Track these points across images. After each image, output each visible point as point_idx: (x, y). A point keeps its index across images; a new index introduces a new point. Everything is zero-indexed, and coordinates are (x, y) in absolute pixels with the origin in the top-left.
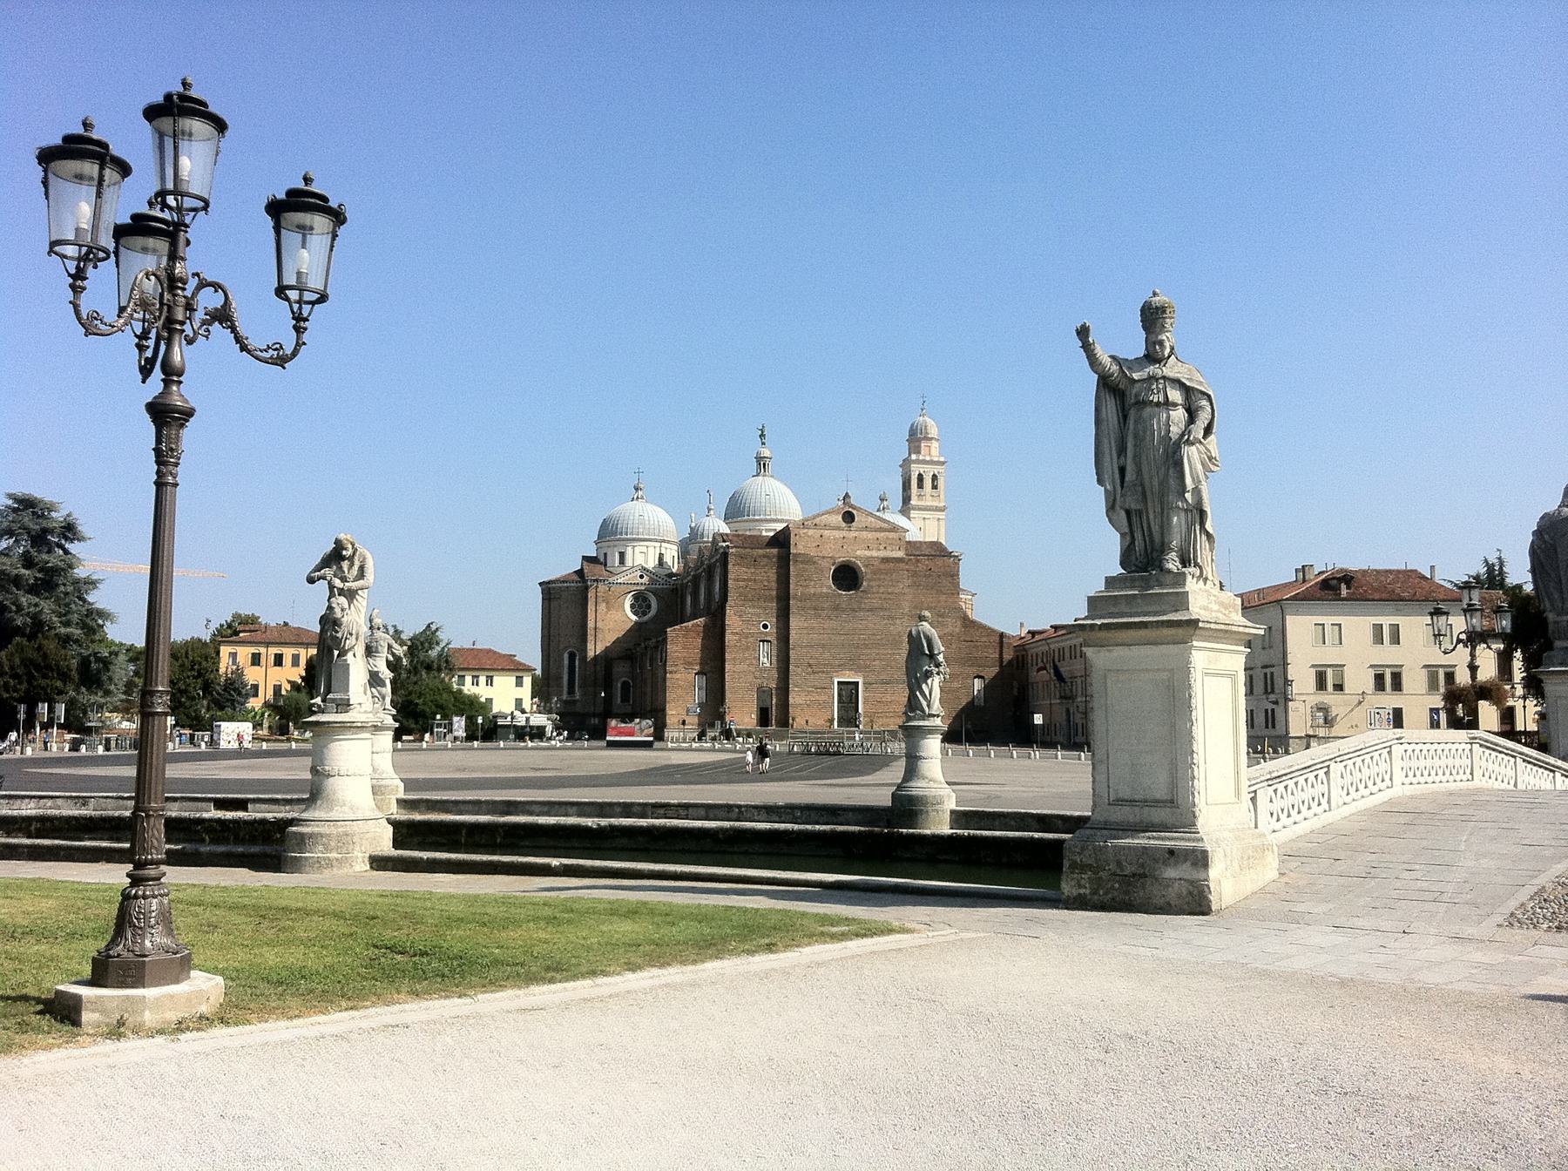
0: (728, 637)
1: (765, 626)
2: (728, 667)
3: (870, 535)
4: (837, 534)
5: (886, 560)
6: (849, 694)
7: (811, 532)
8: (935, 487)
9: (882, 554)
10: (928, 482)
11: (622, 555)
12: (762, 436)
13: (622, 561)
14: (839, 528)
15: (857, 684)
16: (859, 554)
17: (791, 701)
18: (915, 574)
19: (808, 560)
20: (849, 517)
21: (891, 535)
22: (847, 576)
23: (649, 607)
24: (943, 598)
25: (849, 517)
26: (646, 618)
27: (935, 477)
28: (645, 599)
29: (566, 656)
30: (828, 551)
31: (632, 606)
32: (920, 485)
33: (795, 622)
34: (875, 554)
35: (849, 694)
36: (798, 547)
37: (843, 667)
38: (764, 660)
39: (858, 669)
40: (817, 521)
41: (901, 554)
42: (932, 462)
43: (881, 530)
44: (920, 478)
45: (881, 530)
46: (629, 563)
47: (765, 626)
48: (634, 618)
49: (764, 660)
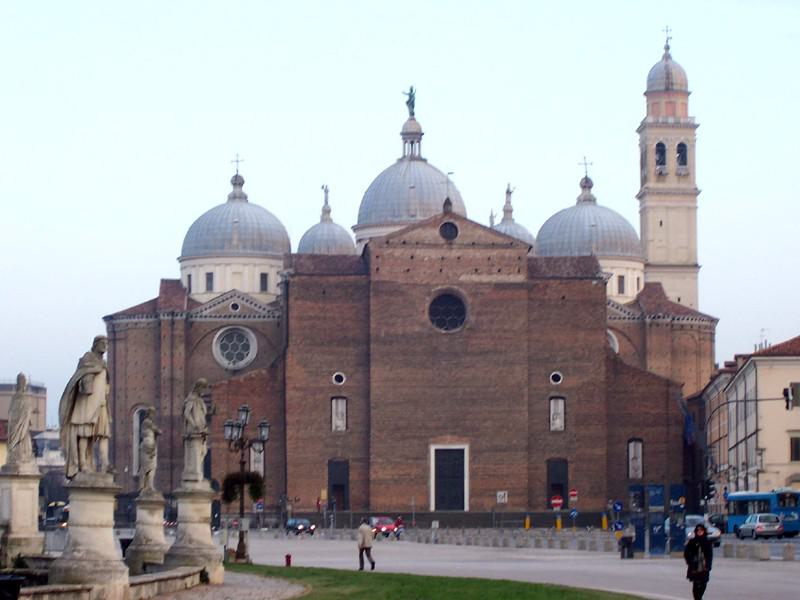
0: (290, 393)
1: (339, 379)
2: (290, 433)
3: (478, 254)
4: (434, 254)
5: (499, 286)
6: (450, 463)
7: (398, 252)
9: (496, 278)
10: (672, 156)
11: (210, 277)
12: (411, 103)
13: (210, 286)
14: (435, 246)
15: (462, 451)
17: (373, 476)
19: (394, 290)
21: (508, 253)
22: (448, 308)
23: (247, 347)
24: (581, 335)
26: (241, 364)
27: (682, 149)
28: (241, 337)
29: (136, 417)
30: (421, 276)
31: (223, 348)
32: (661, 161)
33: (377, 372)
34: (485, 278)
35: (450, 463)
36: (383, 273)
37: (439, 431)
38: (339, 423)
39: (461, 433)
40: (406, 237)
41: (520, 278)
42: (677, 125)
43: (493, 245)
44: (661, 149)
45: (493, 245)
46: (219, 287)
47: (339, 379)
48: (225, 362)
49: (339, 423)
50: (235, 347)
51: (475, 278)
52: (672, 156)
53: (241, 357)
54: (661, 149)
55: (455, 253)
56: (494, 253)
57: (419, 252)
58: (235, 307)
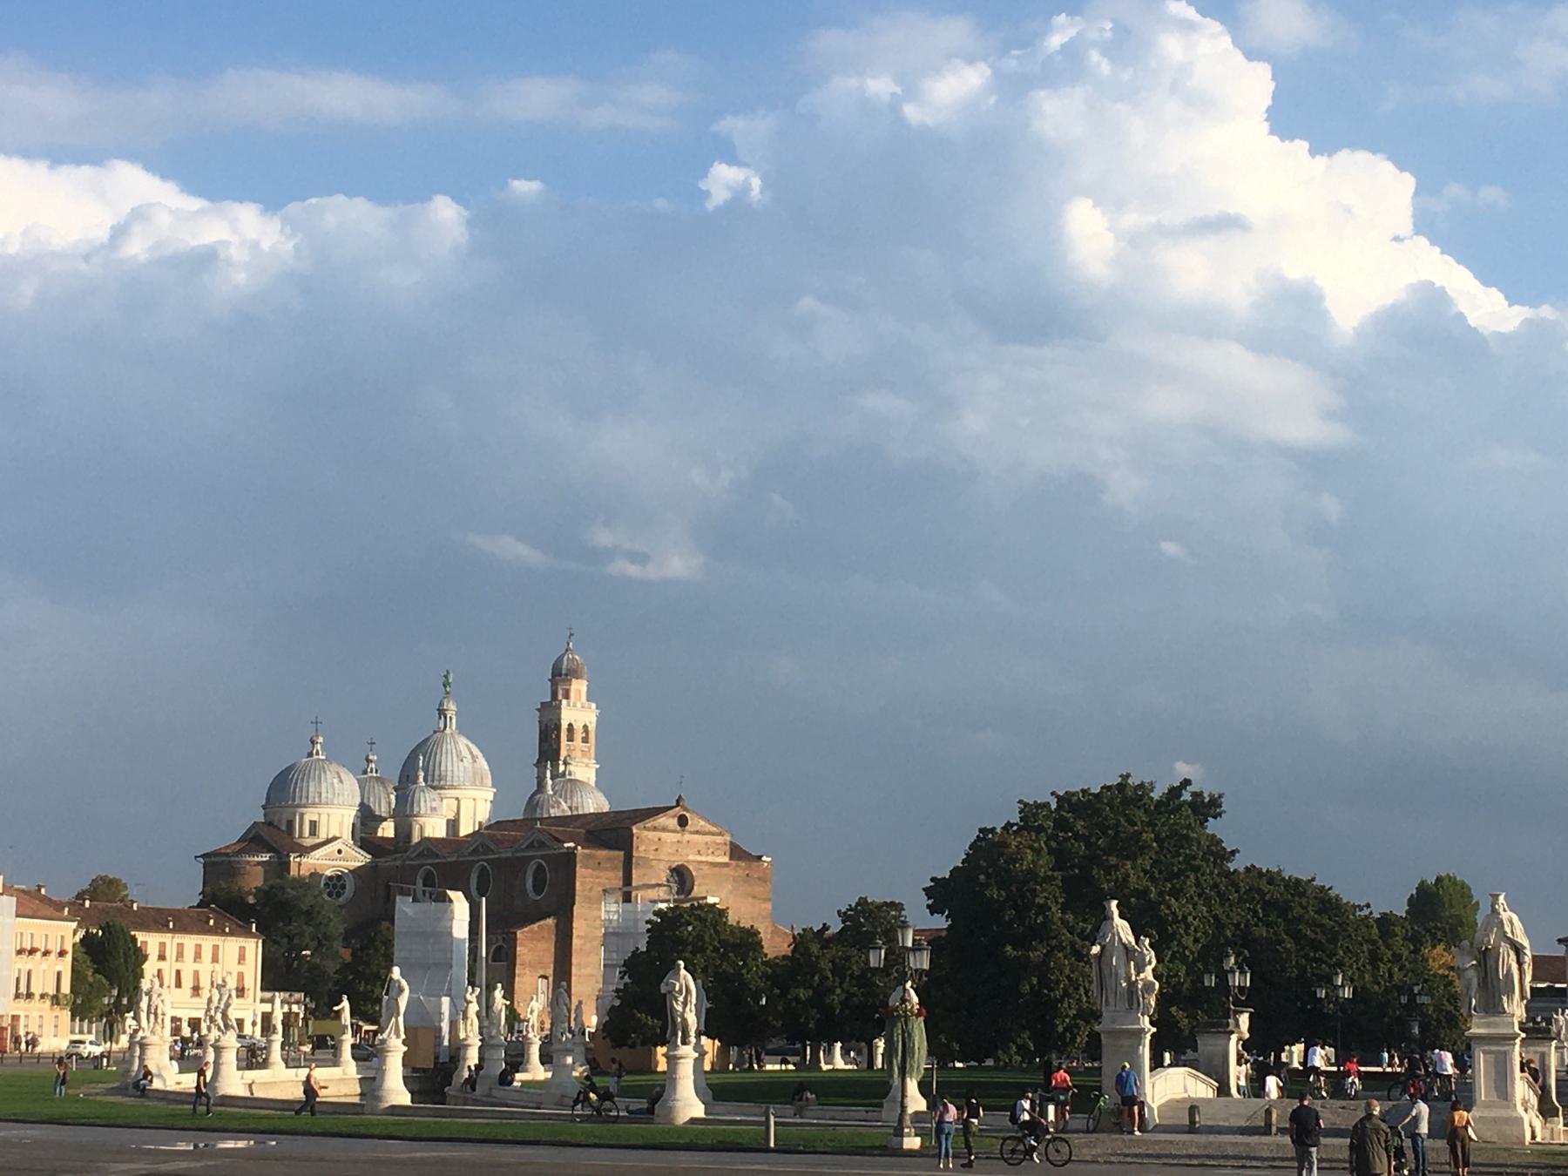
7: (651, 834)
8: (585, 740)
9: (710, 859)
10: (579, 735)
11: (313, 824)
13: (313, 832)
14: (675, 831)
16: (690, 858)
18: (735, 880)
20: (683, 821)
21: (719, 839)
25: (683, 821)
32: (571, 739)
34: (703, 858)
36: (640, 850)
41: (726, 859)
50: (335, 886)
51: (699, 858)
52: (579, 735)
53: (339, 895)
54: (570, 725)
55: (687, 837)
56: (709, 838)
57: (664, 835)
58: (340, 852)
